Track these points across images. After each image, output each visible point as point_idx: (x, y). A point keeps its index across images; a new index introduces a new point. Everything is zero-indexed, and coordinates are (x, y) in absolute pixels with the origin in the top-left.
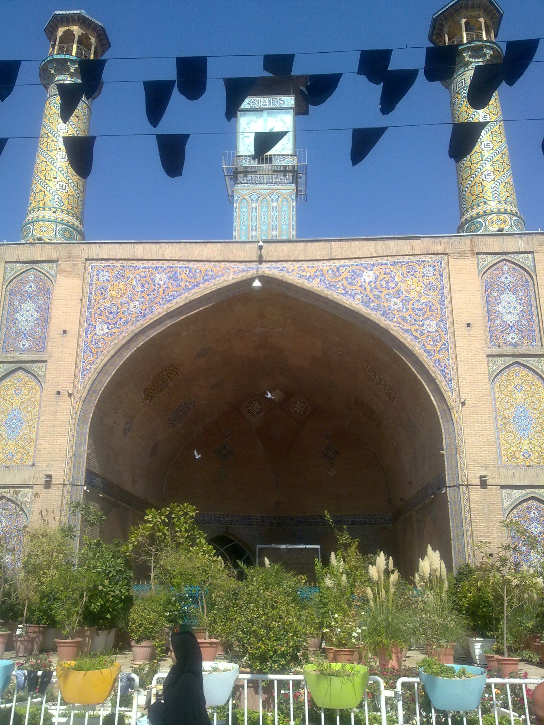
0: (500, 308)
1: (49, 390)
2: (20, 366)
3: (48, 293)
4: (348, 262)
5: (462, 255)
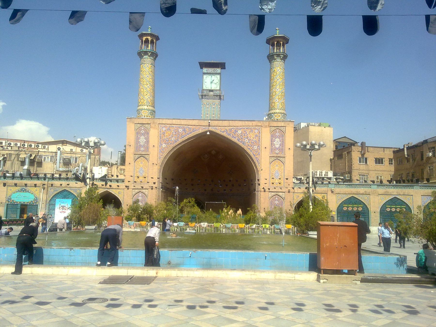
0: (275, 143)
1: (150, 163)
2: (142, 156)
3: (148, 134)
4: (234, 128)
5: (266, 127)
